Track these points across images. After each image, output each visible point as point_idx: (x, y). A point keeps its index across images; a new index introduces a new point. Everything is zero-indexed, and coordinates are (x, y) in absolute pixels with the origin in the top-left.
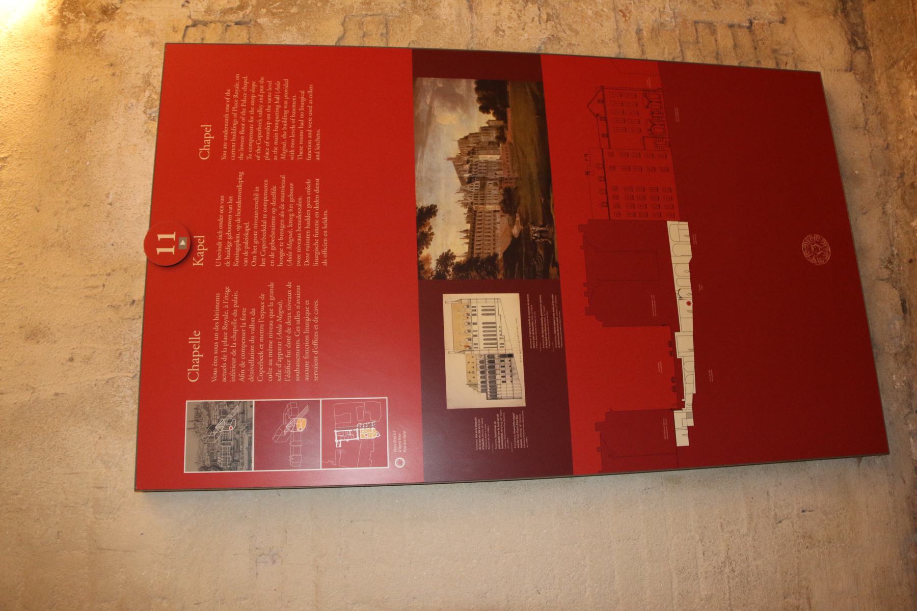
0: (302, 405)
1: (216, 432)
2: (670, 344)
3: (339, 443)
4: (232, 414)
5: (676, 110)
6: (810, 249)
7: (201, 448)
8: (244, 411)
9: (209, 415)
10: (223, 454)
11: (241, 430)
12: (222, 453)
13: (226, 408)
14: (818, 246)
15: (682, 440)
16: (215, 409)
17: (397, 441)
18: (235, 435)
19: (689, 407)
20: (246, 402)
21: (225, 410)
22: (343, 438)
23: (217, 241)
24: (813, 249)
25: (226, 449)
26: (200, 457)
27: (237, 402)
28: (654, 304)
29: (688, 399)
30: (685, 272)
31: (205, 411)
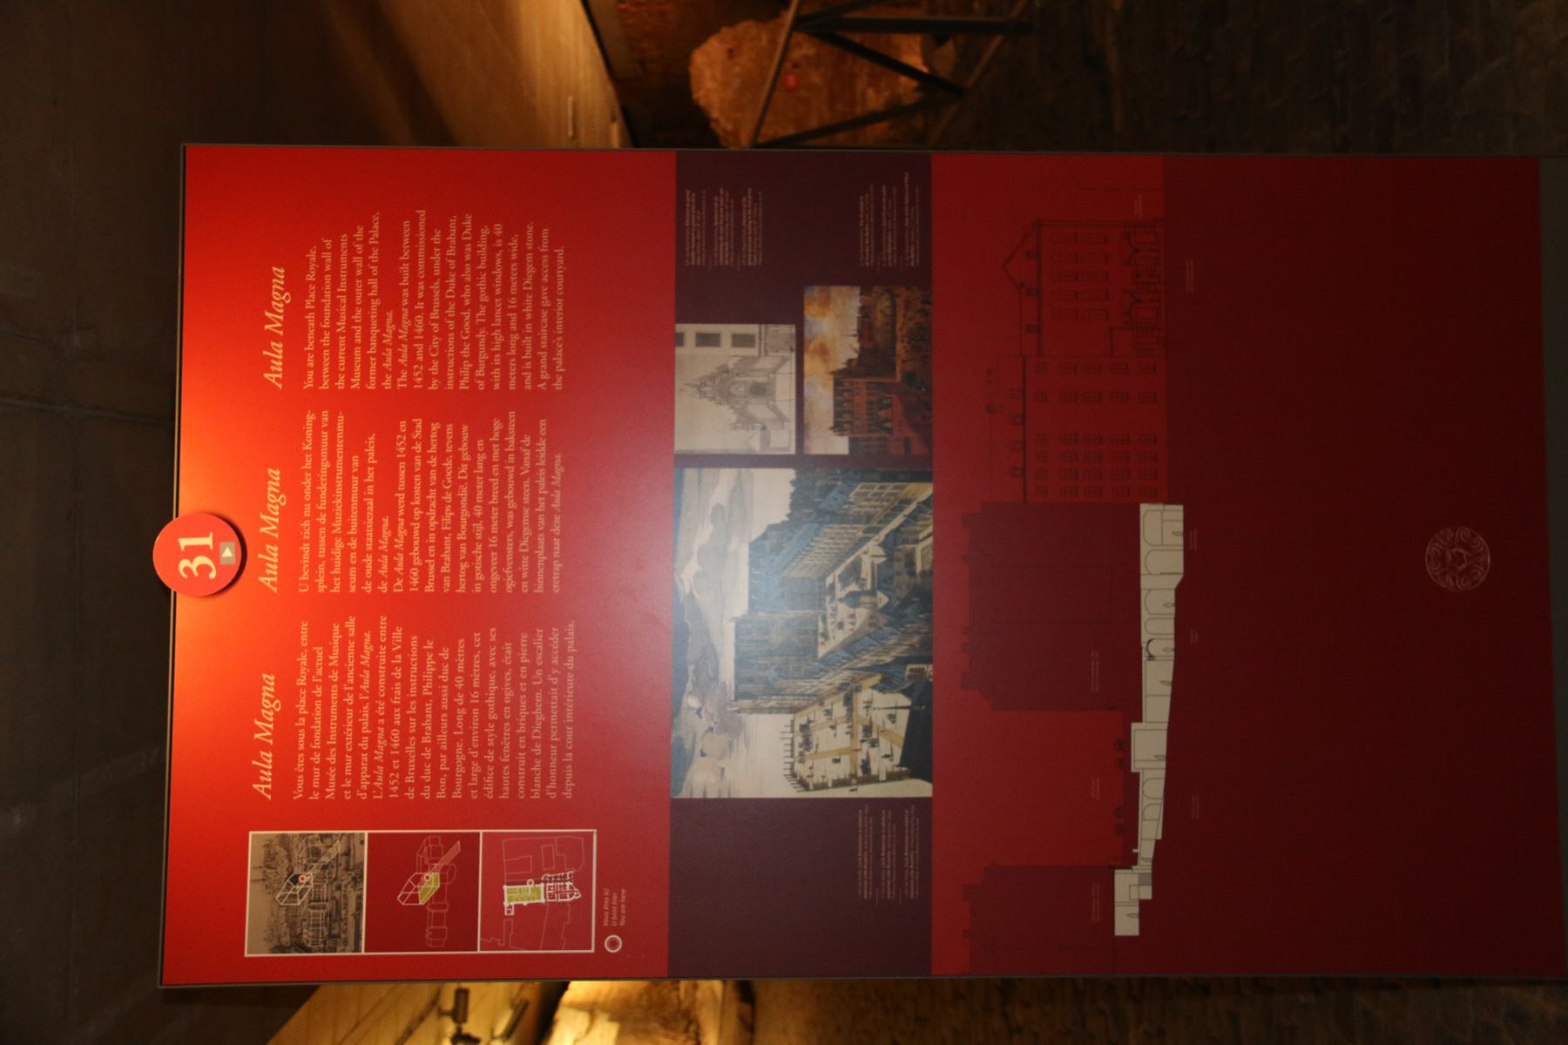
0: (449, 839)
1: (302, 887)
3: (510, 907)
4: (329, 856)
6: (1443, 559)
7: (275, 913)
8: (349, 850)
9: (289, 857)
10: (313, 925)
12: (311, 923)
13: (318, 844)
14: (1462, 551)
15: (1126, 924)
16: (300, 846)
17: (611, 906)
18: (333, 892)
19: (1145, 864)
20: (353, 834)
21: (317, 848)
22: (517, 900)
23: (301, 541)
25: (318, 916)
26: (272, 930)
27: (337, 835)
30: (1165, 605)
31: (282, 849)
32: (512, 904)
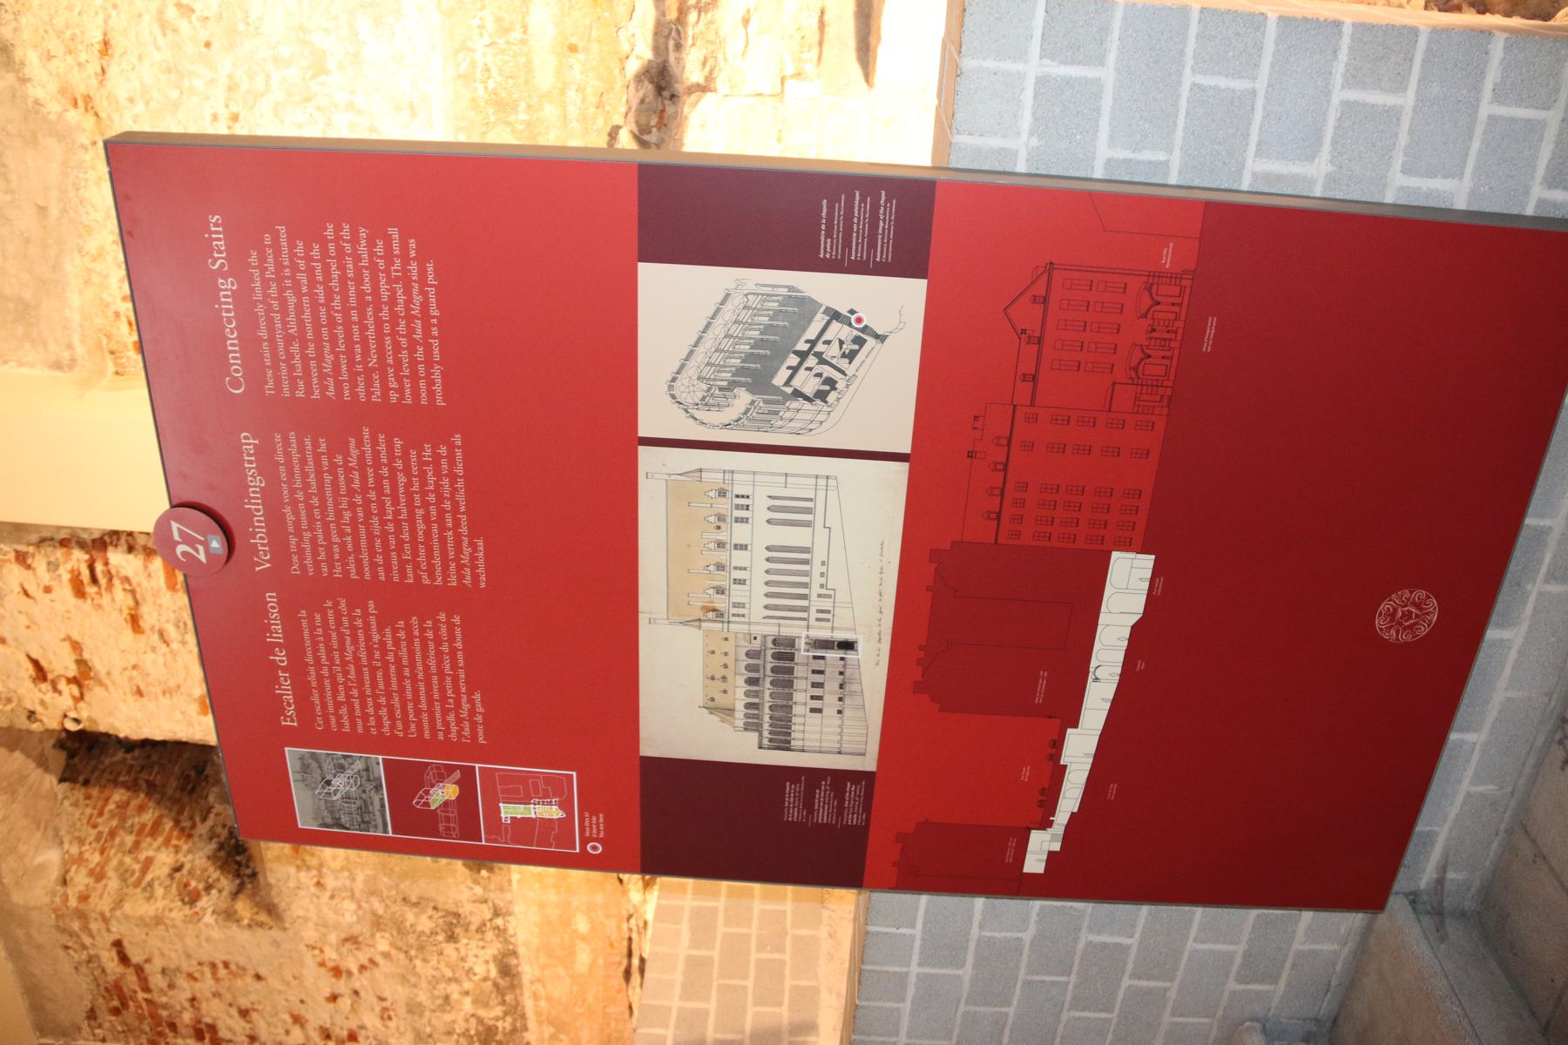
2: (1054, 744)
5: (1212, 322)
9: (320, 767)
11: (367, 789)
13: (342, 761)
15: (1034, 863)
17: (591, 824)
24: (1400, 614)
28: (1042, 684)
29: (1061, 817)
32: (509, 816)
